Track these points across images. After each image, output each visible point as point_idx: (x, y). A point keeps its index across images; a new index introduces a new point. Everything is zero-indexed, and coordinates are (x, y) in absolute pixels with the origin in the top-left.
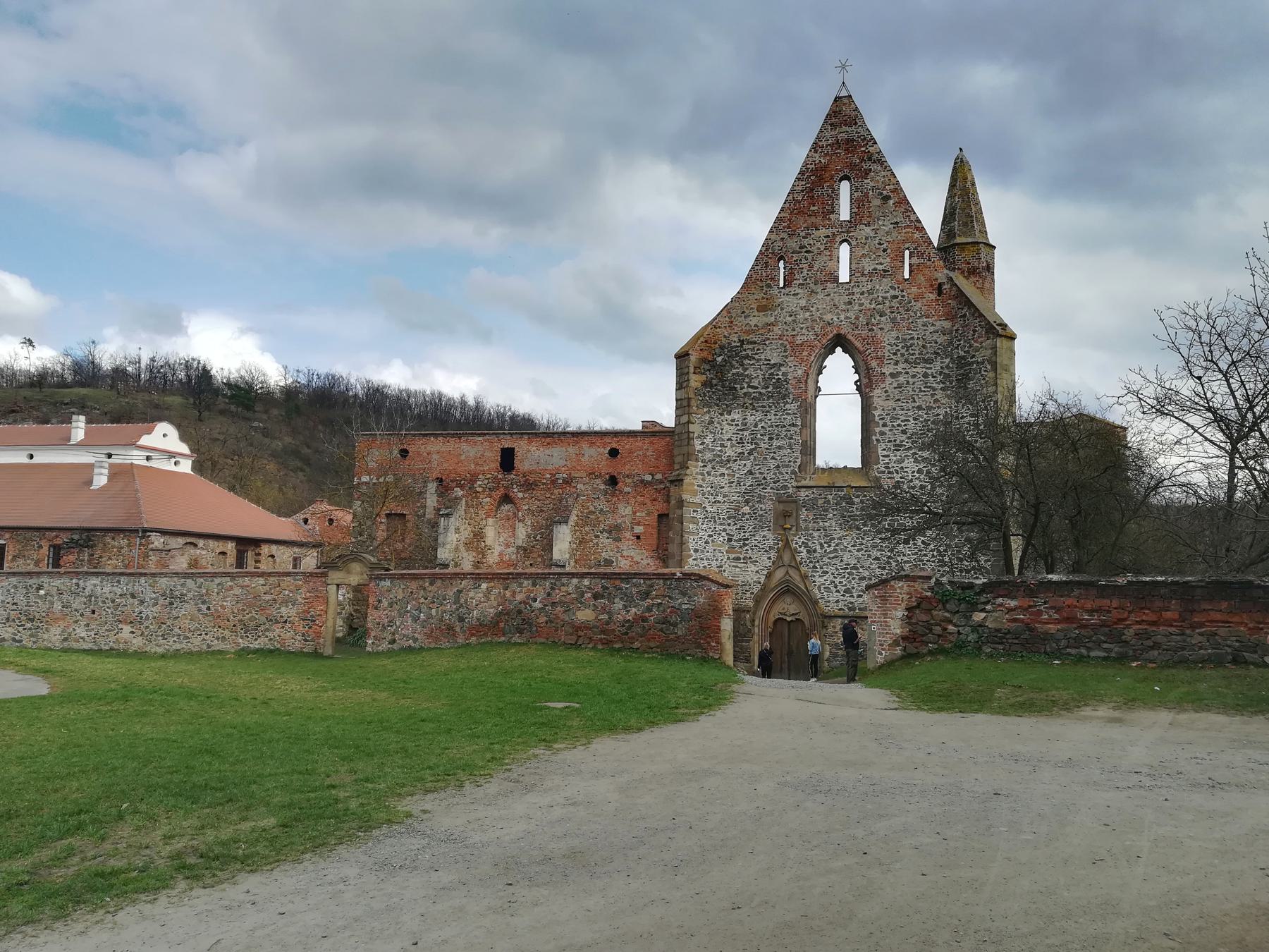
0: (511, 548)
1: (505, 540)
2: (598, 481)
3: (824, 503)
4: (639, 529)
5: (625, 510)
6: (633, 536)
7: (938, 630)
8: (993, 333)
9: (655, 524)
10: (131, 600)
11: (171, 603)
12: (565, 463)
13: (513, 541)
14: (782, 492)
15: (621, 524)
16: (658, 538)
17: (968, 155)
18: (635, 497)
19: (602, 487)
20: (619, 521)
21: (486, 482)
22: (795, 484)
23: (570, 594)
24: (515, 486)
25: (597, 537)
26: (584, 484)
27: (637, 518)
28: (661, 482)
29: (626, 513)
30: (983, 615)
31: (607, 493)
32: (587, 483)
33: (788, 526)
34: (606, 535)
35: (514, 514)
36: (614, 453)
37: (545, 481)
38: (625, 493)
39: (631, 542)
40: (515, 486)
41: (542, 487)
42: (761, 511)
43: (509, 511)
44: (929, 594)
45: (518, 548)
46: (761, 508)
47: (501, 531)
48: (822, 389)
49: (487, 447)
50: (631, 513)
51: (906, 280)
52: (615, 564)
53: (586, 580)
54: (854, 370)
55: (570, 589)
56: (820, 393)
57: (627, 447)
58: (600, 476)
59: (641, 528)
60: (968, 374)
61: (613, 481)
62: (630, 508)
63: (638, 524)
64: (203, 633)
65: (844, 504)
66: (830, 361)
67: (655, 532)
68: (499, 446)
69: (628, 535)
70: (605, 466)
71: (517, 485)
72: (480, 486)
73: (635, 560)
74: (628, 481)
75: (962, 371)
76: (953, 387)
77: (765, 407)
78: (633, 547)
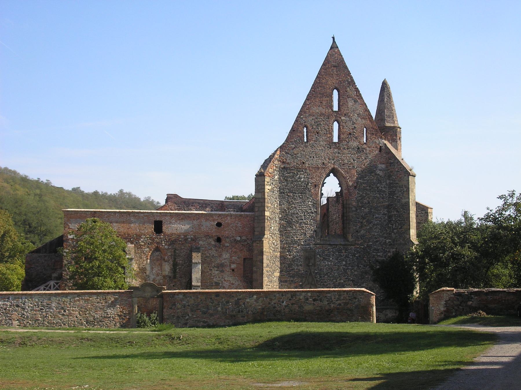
0: (160, 277)
1: (156, 272)
2: (211, 240)
3: (328, 253)
4: (233, 266)
5: (226, 256)
6: (231, 269)
9: (242, 263)
12: (192, 229)
13: (161, 273)
14: (308, 247)
15: (224, 263)
16: (244, 271)
17: (389, 83)
18: (231, 249)
19: (213, 243)
20: (223, 261)
21: (146, 239)
22: (314, 243)
23: (301, 299)
24: (163, 242)
25: (211, 270)
26: (203, 241)
27: (232, 260)
28: (245, 241)
29: (227, 257)
30: (471, 302)
31: (216, 246)
32: (205, 241)
33: (311, 264)
34: (216, 269)
35: (161, 257)
36: (219, 225)
37: (181, 240)
38: (226, 246)
39: (229, 273)
40: (163, 242)
41: (179, 242)
42: (297, 256)
43: (158, 256)
44: (453, 296)
45: (164, 277)
46: (297, 255)
47: (154, 267)
49: (146, 220)
50: (229, 257)
51: (365, 143)
52: (221, 284)
53: (309, 293)
54: (339, 186)
55: (301, 297)
57: (226, 222)
58: (212, 237)
59: (235, 265)
60: (394, 192)
61: (219, 240)
62: (229, 255)
63: (234, 263)
66: (327, 180)
67: (242, 267)
68: (153, 219)
69: (228, 269)
70: (215, 232)
71: (165, 242)
72: (142, 242)
73: (231, 282)
74: (228, 240)
75: (391, 190)
76: (386, 197)
78: (231, 275)
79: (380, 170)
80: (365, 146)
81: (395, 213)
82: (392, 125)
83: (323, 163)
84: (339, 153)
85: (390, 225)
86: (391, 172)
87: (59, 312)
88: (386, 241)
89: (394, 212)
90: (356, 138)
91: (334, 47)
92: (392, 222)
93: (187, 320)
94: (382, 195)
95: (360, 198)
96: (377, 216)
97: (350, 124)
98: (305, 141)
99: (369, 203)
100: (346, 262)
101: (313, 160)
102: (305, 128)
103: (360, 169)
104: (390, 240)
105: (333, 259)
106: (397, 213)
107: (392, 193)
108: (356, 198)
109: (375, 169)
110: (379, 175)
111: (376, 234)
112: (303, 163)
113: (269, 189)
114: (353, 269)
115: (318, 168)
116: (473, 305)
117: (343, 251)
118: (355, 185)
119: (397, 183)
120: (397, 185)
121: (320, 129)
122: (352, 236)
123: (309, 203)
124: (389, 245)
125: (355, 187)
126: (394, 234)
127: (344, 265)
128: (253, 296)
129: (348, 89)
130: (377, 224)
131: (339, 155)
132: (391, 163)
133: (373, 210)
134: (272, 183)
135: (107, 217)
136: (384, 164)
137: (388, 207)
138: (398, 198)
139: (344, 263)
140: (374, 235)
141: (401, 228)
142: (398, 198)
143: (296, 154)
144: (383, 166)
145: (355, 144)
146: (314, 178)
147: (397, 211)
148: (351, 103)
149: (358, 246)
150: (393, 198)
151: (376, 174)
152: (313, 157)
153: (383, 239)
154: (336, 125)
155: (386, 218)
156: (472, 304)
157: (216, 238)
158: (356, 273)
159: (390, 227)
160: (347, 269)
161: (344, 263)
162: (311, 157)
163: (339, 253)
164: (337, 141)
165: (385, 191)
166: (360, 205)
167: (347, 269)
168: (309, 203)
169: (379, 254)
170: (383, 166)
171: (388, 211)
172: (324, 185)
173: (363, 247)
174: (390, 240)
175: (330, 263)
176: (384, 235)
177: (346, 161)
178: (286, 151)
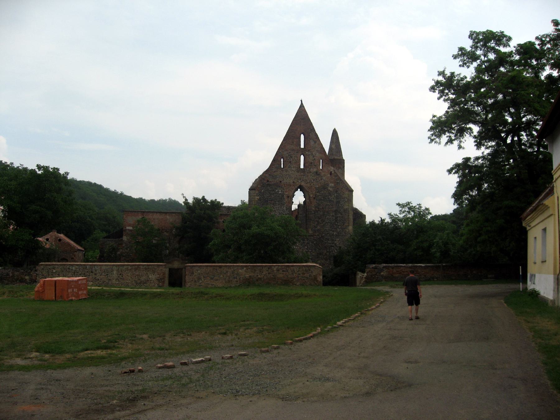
7: (374, 276)
8: (348, 190)
10: (91, 274)
11: (107, 275)
48: (294, 202)
54: (304, 197)
56: (293, 204)
64: (121, 285)
65: (302, 241)
66: (296, 193)
75: (337, 200)
77: (277, 208)
79: (330, 187)
80: (321, 171)
81: (340, 215)
82: (339, 158)
83: (294, 182)
84: (304, 175)
85: (336, 223)
86: (337, 189)
87: (119, 277)
88: (333, 233)
89: (339, 214)
90: (315, 166)
91: (302, 106)
92: (338, 221)
93: (201, 283)
94: (332, 203)
95: (317, 205)
96: (328, 217)
97: (311, 157)
98: (282, 167)
99: (323, 208)
100: (307, 247)
101: (287, 180)
102: (282, 159)
103: (317, 186)
104: (336, 233)
105: (299, 244)
106: (341, 215)
107: (338, 202)
108: (315, 205)
109: (327, 187)
110: (330, 190)
111: (327, 229)
112: (281, 182)
113: (257, 199)
114: (312, 251)
115: (290, 185)
116: (384, 275)
117: (306, 240)
118: (314, 197)
119: (341, 196)
120: (341, 197)
121: (292, 160)
122: (312, 230)
123: (285, 208)
124: (336, 236)
125: (314, 198)
126: (339, 229)
127: (306, 249)
128: (243, 268)
129: (310, 134)
130: (329, 222)
131: (304, 177)
132: (337, 183)
133: (325, 213)
134: (260, 195)
135: (151, 216)
136: (333, 183)
137: (336, 212)
138: (342, 206)
139: (306, 247)
140: (326, 229)
141: (343, 225)
142: (342, 206)
143: (276, 176)
144: (333, 185)
145: (315, 170)
146: (287, 192)
147: (341, 214)
148: (312, 143)
149: (315, 237)
150: (339, 205)
151: (328, 190)
152: (287, 178)
153: (332, 232)
154: (302, 157)
155: (334, 218)
156: (383, 274)
157: (223, 230)
158: (314, 254)
159: (336, 224)
160: (308, 251)
161: (306, 247)
162: (286, 178)
163: (303, 241)
164: (303, 168)
165: (333, 201)
166: (317, 209)
167: (308, 251)
168: (285, 208)
169: (329, 242)
170: (333, 185)
171: (335, 214)
172: (294, 196)
173: (318, 237)
174: (336, 233)
175: (297, 247)
176: (333, 230)
177: (308, 181)
178: (270, 173)
